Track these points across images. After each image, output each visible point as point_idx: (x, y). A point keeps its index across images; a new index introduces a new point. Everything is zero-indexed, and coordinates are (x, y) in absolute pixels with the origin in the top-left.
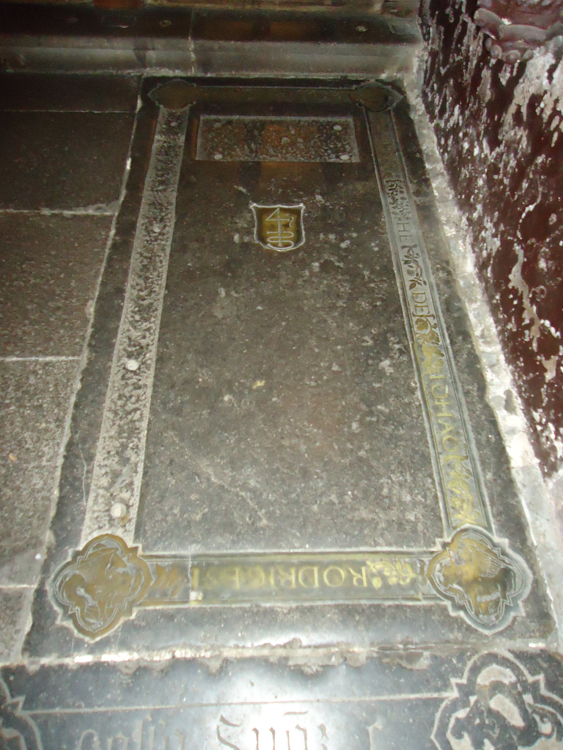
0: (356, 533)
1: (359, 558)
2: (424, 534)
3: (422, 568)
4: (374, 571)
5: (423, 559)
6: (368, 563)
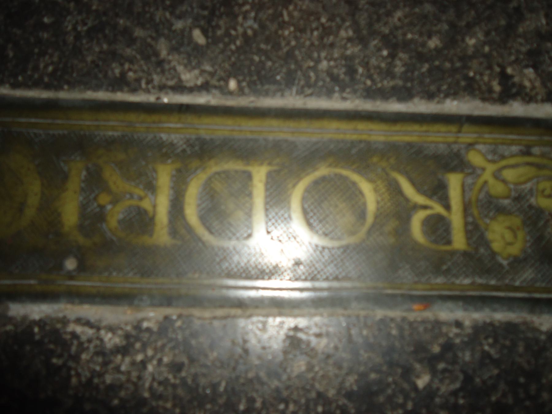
0: (433, 43)
1: (438, 138)
4: (497, 188)
6: (475, 158)
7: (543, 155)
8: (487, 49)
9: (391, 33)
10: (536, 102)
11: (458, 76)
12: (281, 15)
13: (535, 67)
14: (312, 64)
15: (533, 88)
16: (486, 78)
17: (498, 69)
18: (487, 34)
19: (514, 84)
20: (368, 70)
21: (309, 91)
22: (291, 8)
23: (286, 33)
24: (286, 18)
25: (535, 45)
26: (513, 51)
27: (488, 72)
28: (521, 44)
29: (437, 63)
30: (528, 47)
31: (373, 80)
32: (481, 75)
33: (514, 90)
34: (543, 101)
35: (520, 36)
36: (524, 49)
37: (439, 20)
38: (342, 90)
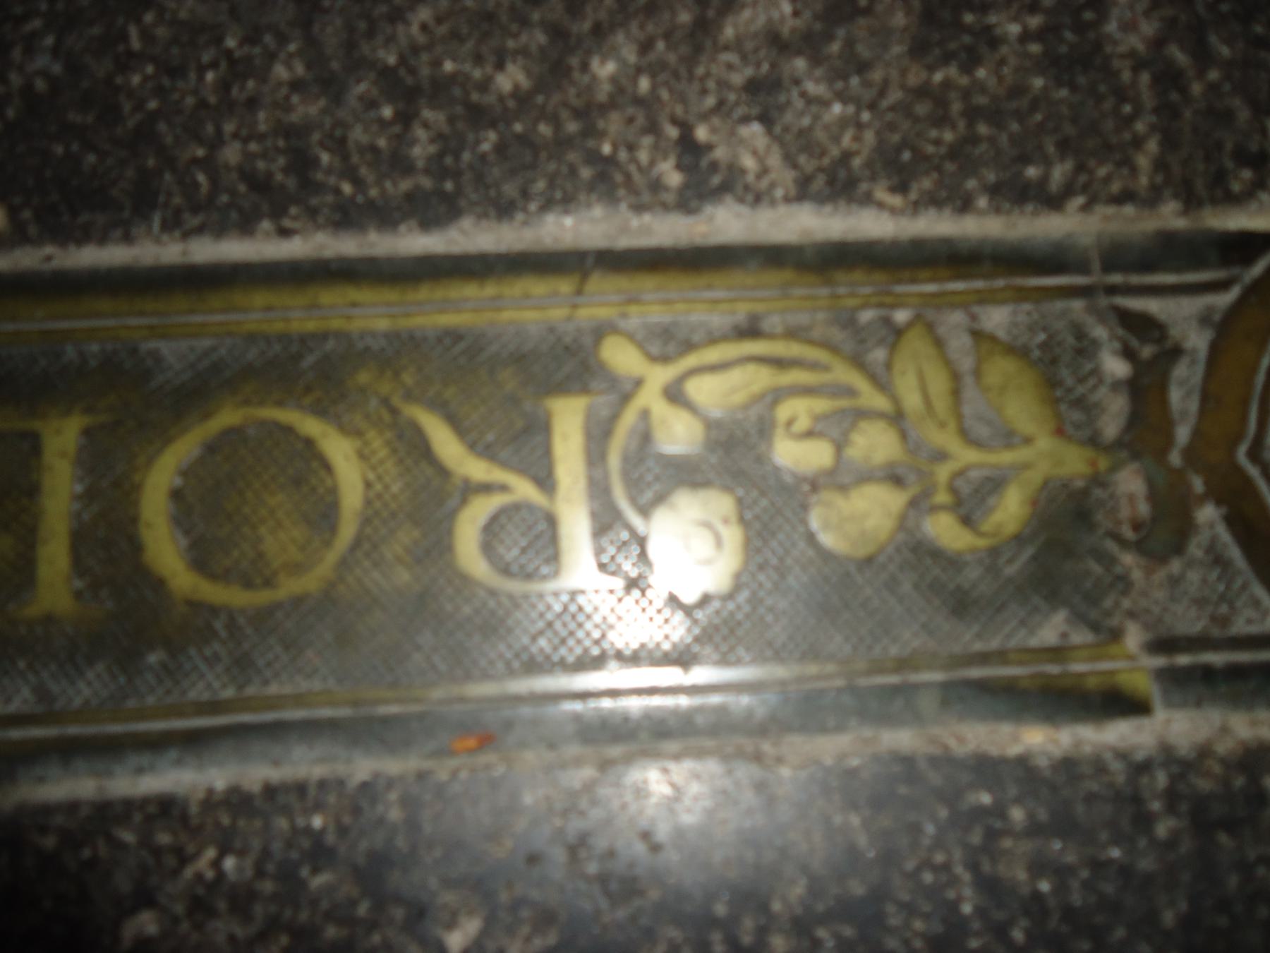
0: (511, 78)
2: (1169, 78)
3: (1146, 388)
5: (1152, 306)
6: (621, 356)
7: (792, 334)
8: (644, 84)
9: (402, 60)
10: (773, 203)
11: (572, 156)
12: (124, 37)
13: (766, 119)
14: (200, 152)
15: (764, 171)
16: (643, 156)
17: (673, 132)
18: (646, 47)
19: (714, 166)
20: (345, 157)
21: (194, 221)
22: (149, 18)
23: (136, 79)
24: (136, 44)
25: (765, 67)
26: (711, 84)
27: (647, 141)
28: (730, 67)
29: (518, 127)
30: (749, 72)
31: (358, 182)
32: (631, 148)
33: (716, 180)
34: (787, 200)
35: (726, 48)
36: (737, 79)
37: (524, 22)
38: (278, 213)
